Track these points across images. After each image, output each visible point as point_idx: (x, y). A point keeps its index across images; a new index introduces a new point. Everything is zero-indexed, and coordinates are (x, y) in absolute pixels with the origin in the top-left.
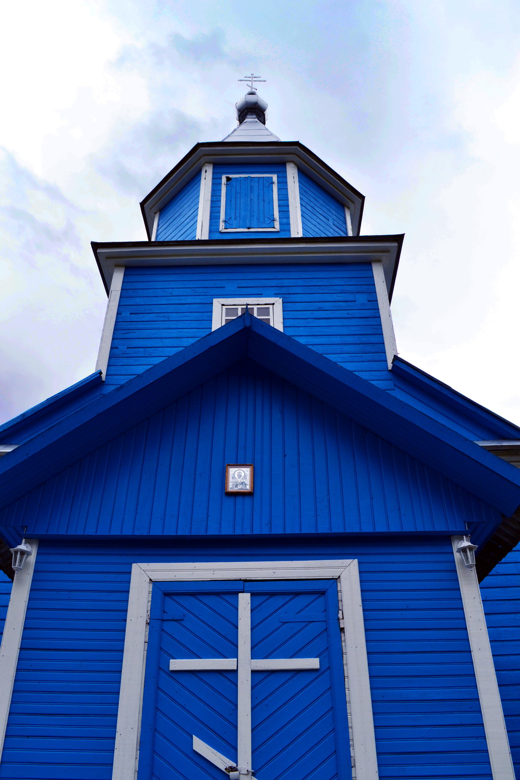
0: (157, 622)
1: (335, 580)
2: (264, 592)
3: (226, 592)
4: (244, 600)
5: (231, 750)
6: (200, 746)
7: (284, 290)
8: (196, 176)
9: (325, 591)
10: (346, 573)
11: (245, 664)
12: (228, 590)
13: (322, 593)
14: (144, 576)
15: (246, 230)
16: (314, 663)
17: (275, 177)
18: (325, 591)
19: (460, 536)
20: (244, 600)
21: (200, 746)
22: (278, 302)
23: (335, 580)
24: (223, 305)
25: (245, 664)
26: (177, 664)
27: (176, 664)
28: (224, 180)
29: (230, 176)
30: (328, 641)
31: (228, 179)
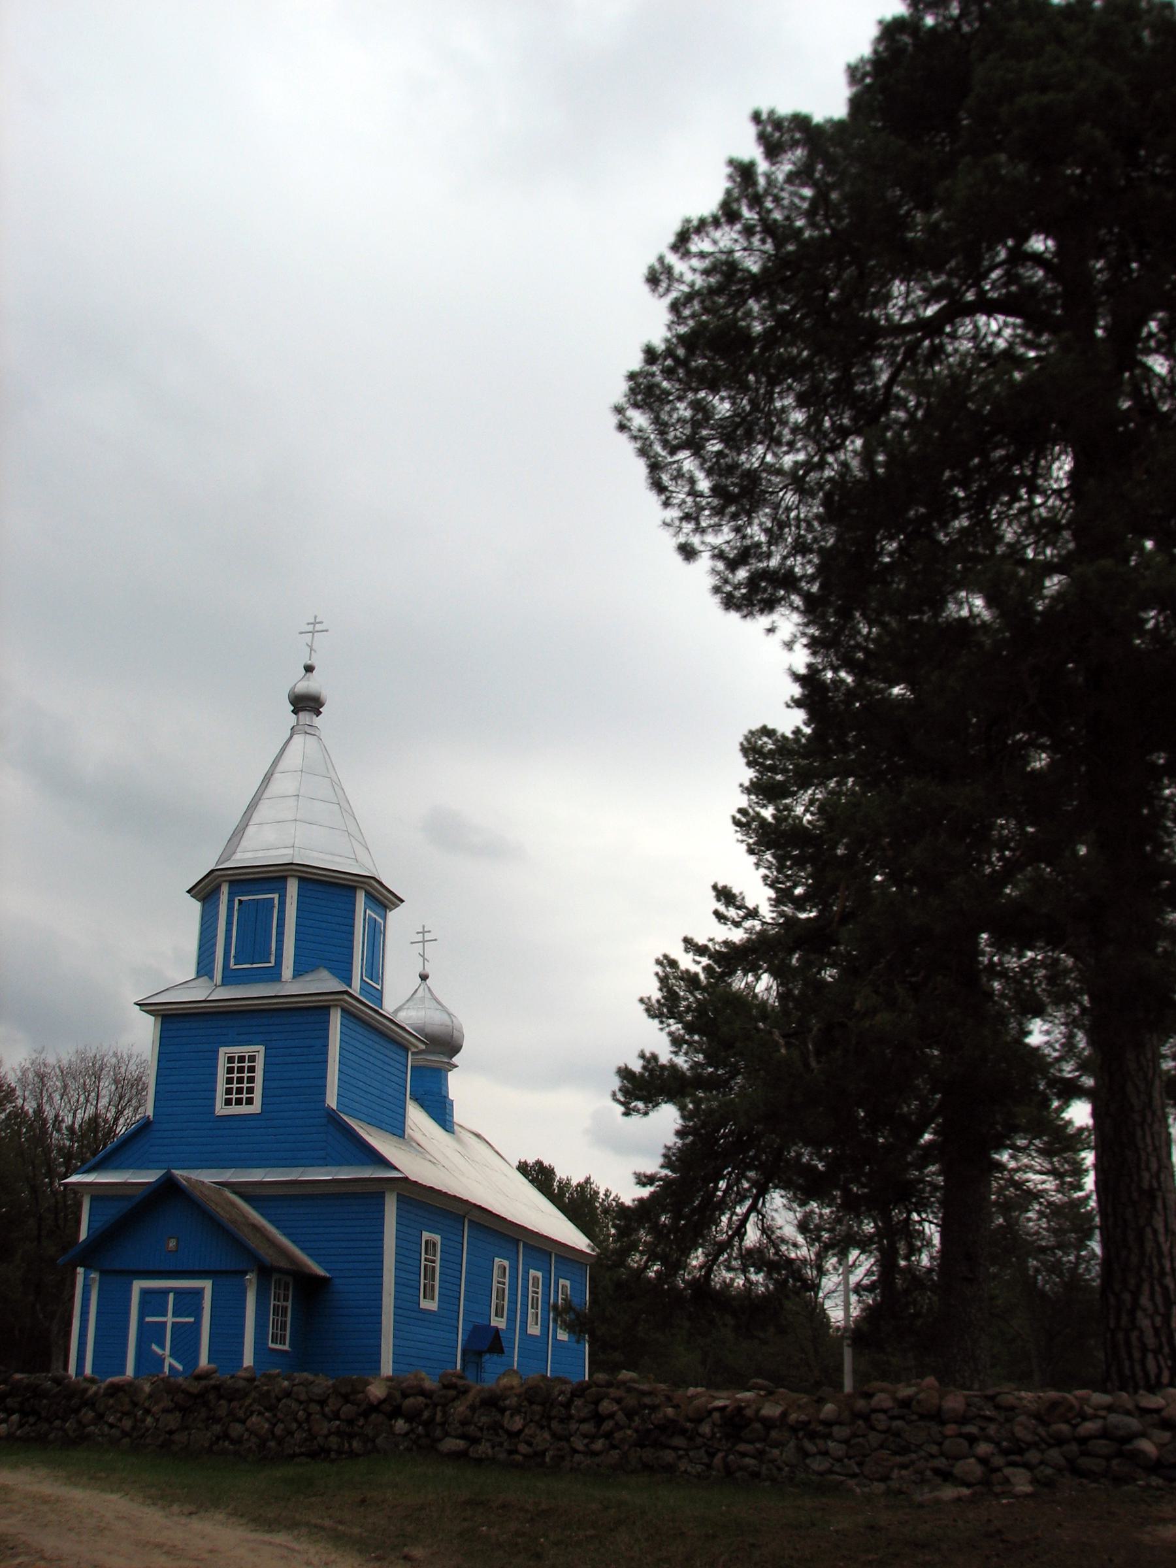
1: (204, 1288)
2: (178, 1292)
4: (171, 1295)
8: (219, 887)
9: (199, 1293)
10: (207, 1285)
11: (169, 1319)
12: (165, 1292)
14: (138, 1285)
16: (192, 1320)
17: (276, 896)
18: (199, 1293)
19: (252, 1271)
20: (171, 1295)
22: (262, 1048)
23: (204, 1288)
25: (169, 1319)
26: (148, 1319)
27: (148, 1319)
28: (237, 902)
30: (197, 1313)
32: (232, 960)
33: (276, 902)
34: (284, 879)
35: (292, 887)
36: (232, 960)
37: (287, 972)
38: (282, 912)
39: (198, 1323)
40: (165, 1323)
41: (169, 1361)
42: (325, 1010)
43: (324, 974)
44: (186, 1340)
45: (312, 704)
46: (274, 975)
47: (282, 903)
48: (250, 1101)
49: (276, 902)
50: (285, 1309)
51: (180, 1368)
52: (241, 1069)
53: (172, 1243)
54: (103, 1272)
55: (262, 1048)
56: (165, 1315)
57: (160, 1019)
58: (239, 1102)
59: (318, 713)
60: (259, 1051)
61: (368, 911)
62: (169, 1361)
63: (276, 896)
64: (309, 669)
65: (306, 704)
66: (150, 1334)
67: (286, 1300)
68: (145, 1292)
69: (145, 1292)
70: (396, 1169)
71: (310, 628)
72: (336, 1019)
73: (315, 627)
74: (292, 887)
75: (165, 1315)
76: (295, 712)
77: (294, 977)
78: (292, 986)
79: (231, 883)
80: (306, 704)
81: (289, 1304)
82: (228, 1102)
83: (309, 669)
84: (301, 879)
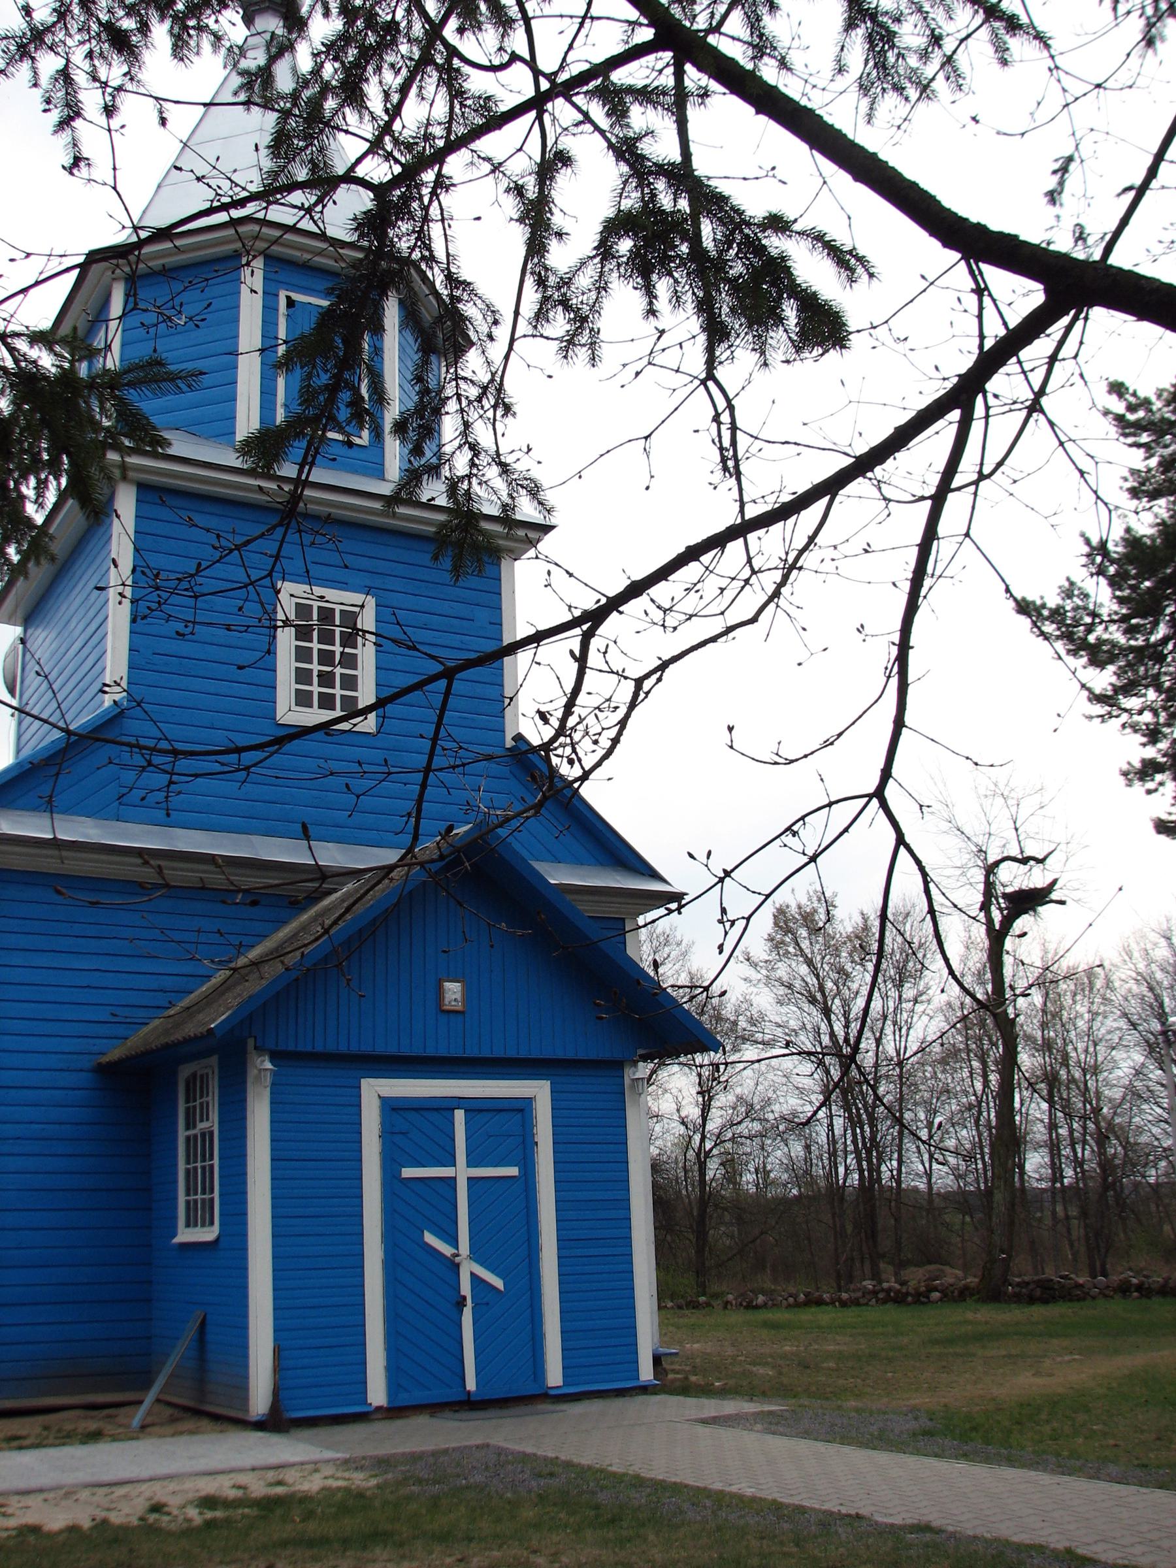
0: (388, 1134)
1: (529, 1101)
2: (476, 1108)
3: (444, 1107)
4: (459, 1115)
5: (454, 1241)
6: (430, 1238)
7: (378, 582)
9: (522, 1109)
10: (539, 1092)
12: (445, 1107)
13: (522, 1110)
14: (374, 1091)
16: (513, 1171)
18: (522, 1109)
20: (459, 1115)
21: (430, 1238)
22: (371, 602)
23: (529, 1101)
24: (292, 595)
25: (462, 1172)
26: (408, 1172)
27: (408, 1172)
29: (296, 297)
31: (291, 303)
41: (468, 1268)
44: (505, 1222)
51: (498, 1283)
53: (453, 991)
54: (275, 1056)
68: (392, 1108)
69: (392, 1108)
70: (655, 875)
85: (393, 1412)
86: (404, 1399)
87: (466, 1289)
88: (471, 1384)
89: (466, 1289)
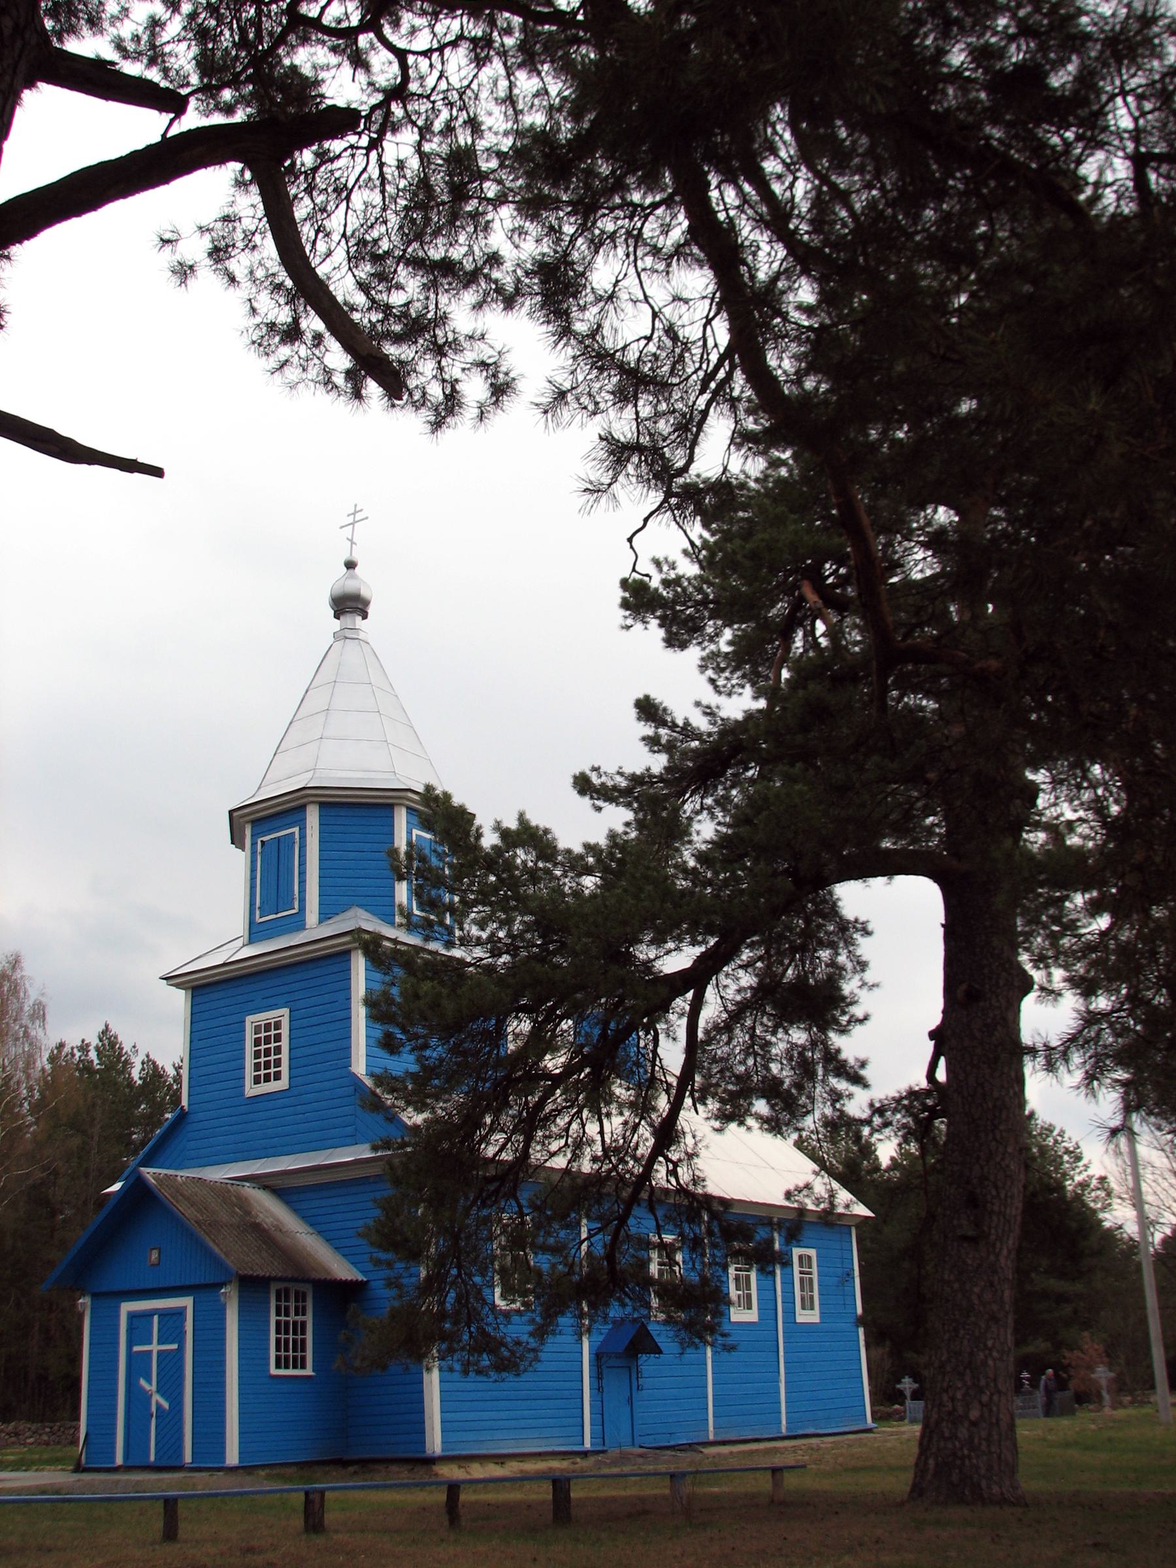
0: (130, 1330)
2: (164, 1314)
4: (156, 1318)
5: (151, 1384)
9: (180, 1313)
10: (186, 1302)
14: (127, 1307)
15: (274, 916)
17: (296, 830)
20: (156, 1318)
22: (285, 1011)
29: (265, 839)
32: (258, 912)
33: (297, 836)
34: (302, 808)
35: (313, 817)
36: (258, 912)
37: (312, 917)
38: (303, 847)
39: (181, 1349)
40: (150, 1352)
42: (345, 955)
43: (361, 913)
45: (349, 604)
46: (298, 923)
47: (303, 837)
48: (278, 1076)
49: (297, 836)
50: (304, 1324)
52: (268, 1037)
53: (155, 1255)
54: (95, 1296)
55: (285, 1011)
56: (160, 1342)
57: (190, 992)
58: (267, 1078)
59: (365, 617)
60: (282, 1014)
61: (415, 832)
62: (156, 1398)
63: (296, 830)
64: (350, 565)
65: (348, 605)
66: (138, 1365)
67: (304, 1314)
68: (132, 1316)
69: (132, 1316)
71: (351, 519)
72: (359, 965)
73: (355, 517)
74: (313, 817)
75: (160, 1342)
76: (337, 616)
77: (320, 922)
78: (315, 928)
79: (254, 822)
80: (348, 605)
81: (309, 1319)
82: (257, 1080)
83: (350, 565)
84: (322, 805)
85: (127, 1468)
86: (130, 1463)
87: (154, 1409)
88: (152, 1458)
89: (154, 1409)
